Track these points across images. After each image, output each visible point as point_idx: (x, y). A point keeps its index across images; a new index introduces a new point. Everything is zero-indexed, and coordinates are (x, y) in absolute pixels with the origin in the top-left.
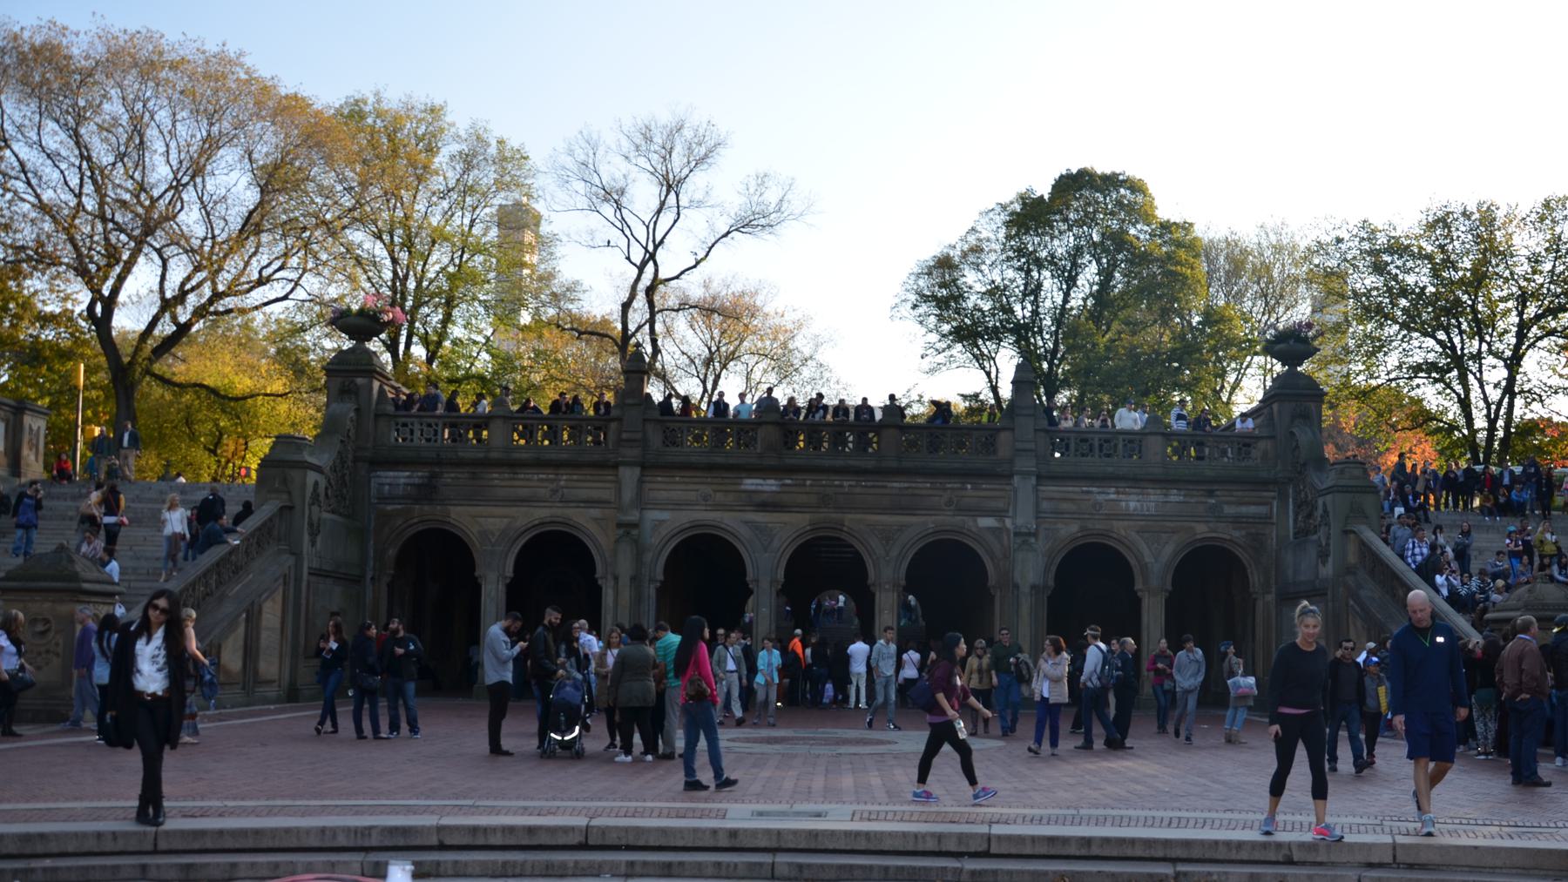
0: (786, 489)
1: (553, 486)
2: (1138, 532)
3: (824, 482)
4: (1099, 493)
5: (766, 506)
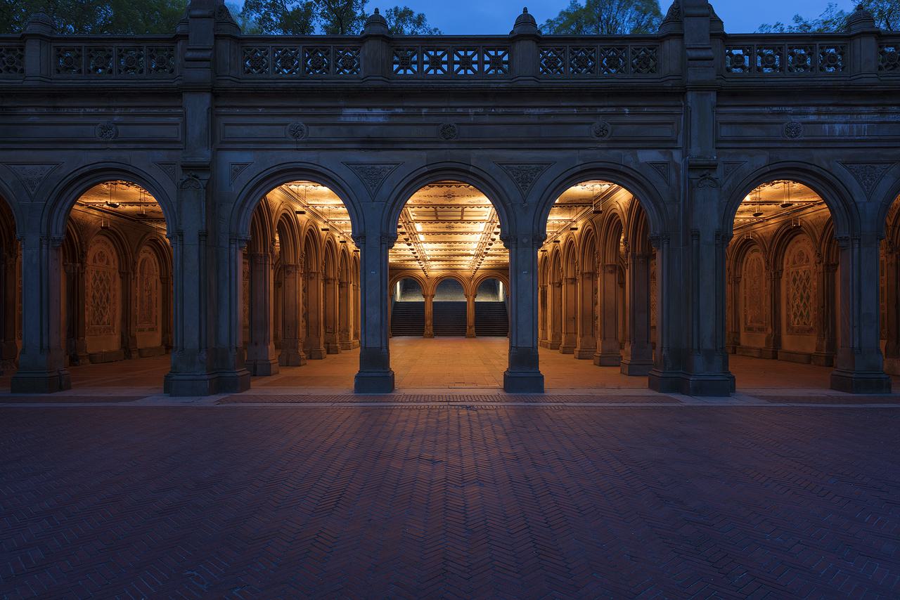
0: (396, 120)
1: (103, 121)
2: (844, 164)
3: (444, 110)
4: (794, 114)
5: (369, 143)
